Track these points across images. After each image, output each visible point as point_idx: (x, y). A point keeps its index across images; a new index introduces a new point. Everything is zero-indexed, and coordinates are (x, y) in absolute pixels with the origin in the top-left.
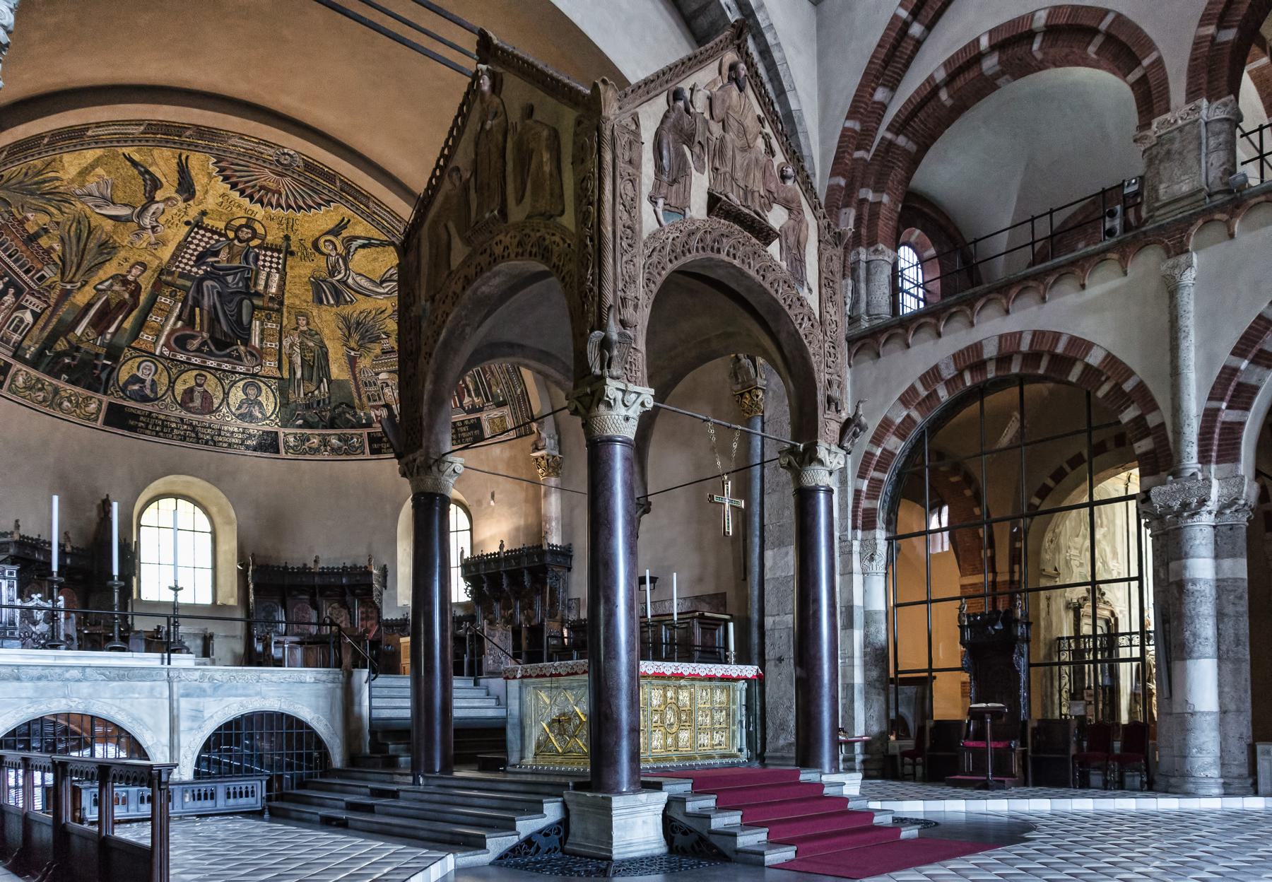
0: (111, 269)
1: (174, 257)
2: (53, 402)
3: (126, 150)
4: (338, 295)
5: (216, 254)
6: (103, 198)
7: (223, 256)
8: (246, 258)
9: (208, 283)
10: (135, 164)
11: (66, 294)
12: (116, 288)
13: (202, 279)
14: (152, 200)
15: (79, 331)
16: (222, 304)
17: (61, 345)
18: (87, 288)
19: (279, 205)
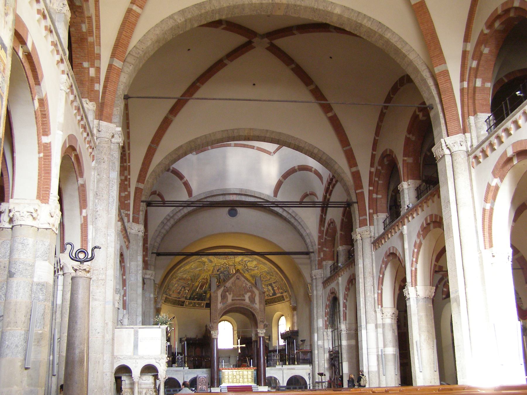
0: (201, 278)
1: (213, 272)
2: (194, 306)
3: (197, 261)
4: (247, 271)
5: (221, 269)
6: (196, 268)
7: (222, 269)
8: (227, 268)
9: (221, 274)
10: (200, 262)
11: (193, 285)
12: (203, 280)
13: (219, 274)
14: (205, 265)
15: (197, 290)
16: (225, 277)
17: (194, 294)
18: (197, 283)
19: (229, 259)
